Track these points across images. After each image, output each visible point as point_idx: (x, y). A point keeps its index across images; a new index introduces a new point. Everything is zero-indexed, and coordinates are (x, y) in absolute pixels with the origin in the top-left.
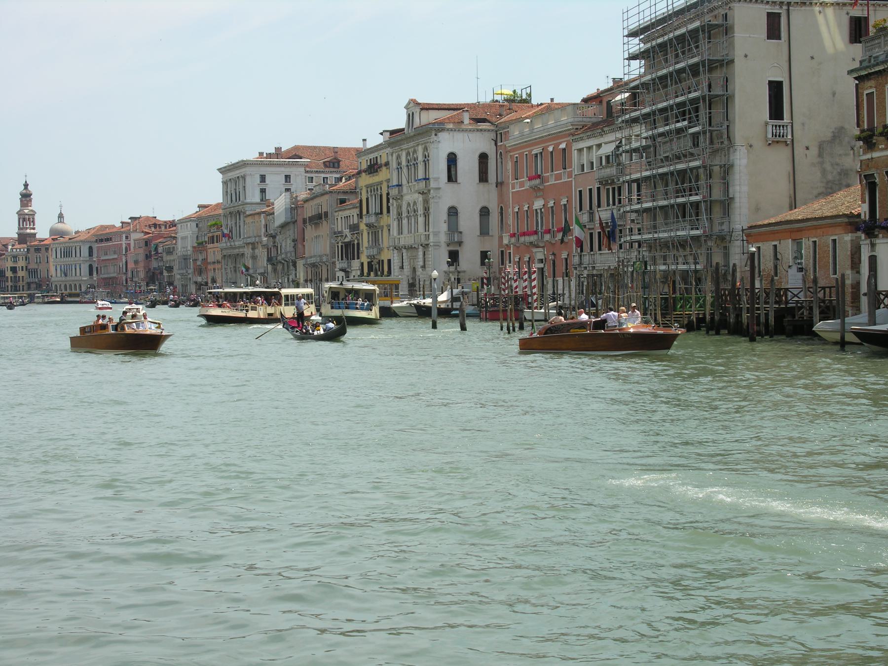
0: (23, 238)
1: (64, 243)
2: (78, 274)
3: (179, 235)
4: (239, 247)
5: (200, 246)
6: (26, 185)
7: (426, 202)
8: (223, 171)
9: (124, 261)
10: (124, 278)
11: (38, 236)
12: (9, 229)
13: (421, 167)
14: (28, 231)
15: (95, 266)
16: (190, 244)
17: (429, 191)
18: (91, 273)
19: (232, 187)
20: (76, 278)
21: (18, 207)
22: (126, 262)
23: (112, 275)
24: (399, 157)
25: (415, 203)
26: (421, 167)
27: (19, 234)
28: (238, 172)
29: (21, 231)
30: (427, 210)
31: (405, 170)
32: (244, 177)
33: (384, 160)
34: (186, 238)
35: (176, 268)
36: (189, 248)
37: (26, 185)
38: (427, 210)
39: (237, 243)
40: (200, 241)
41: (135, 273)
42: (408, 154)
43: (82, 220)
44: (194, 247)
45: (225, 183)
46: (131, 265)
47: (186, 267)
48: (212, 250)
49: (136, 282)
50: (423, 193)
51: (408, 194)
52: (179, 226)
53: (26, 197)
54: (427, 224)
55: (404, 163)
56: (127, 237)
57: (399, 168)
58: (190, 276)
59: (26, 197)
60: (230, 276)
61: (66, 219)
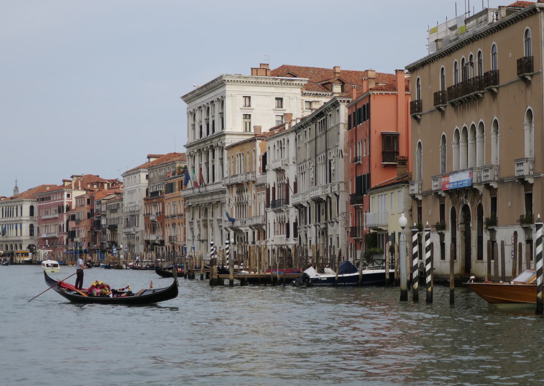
8: (188, 98)
20: (17, 238)
28: (213, 94)
56: (68, 196)
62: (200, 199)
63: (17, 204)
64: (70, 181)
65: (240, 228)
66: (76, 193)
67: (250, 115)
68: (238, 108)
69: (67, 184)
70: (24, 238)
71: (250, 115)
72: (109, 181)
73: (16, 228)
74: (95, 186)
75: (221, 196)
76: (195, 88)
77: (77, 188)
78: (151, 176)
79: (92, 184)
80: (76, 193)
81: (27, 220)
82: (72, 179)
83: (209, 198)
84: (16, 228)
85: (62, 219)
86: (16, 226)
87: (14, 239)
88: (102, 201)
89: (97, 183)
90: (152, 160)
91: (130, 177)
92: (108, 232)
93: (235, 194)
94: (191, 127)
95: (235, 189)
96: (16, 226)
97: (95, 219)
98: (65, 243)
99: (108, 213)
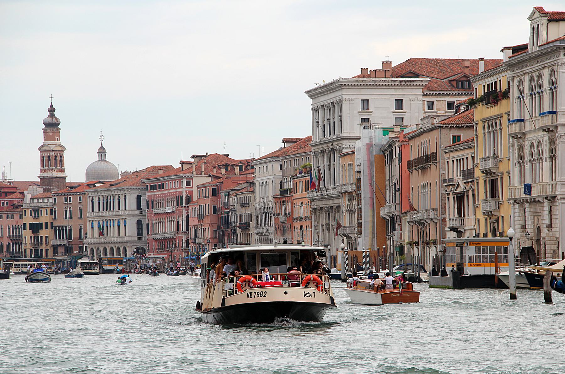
0: (45, 183)
1: (105, 187)
2: (122, 234)
3: (257, 181)
4: (333, 198)
5: (284, 194)
6: (52, 110)
7: (552, 141)
8: (313, 94)
9: (185, 216)
10: (184, 239)
11: (67, 180)
12: (25, 169)
13: (547, 97)
14: (55, 174)
15: (145, 222)
16: (272, 191)
17: (556, 127)
18: (139, 234)
19: (323, 115)
20: (119, 240)
21: (40, 140)
22: (187, 217)
23: (166, 235)
24: (521, 82)
25: (539, 143)
26: (547, 97)
27: (42, 178)
28: (332, 95)
29: (45, 174)
30: (553, 151)
31: (528, 101)
32: (340, 103)
33: (504, 87)
34: (266, 184)
35: (253, 225)
36: (271, 198)
37: (52, 110)
38: (553, 151)
39: (330, 192)
40: (285, 187)
41: (199, 232)
42: (532, 79)
43: (128, 160)
44: (275, 197)
45: (315, 111)
46: (194, 222)
47: (266, 223)
48: (298, 202)
49: (200, 244)
50: (548, 131)
51: (531, 131)
52: (257, 167)
53: (52, 126)
54: (553, 170)
55: (527, 91)
56: (188, 183)
57: (521, 98)
58: (271, 236)
59: (52, 126)
60: (321, 236)
61: (109, 157)
62: (324, 202)
63: (119, 192)
64: (190, 163)
65: (350, 235)
66: (198, 181)
67: (369, 119)
68: (356, 112)
69: (185, 167)
70: (129, 239)
71: (369, 119)
72: (241, 162)
73: (119, 226)
74: (223, 171)
75: (336, 201)
76: (317, 86)
77: (199, 174)
78: (284, 168)
79: (219, 167)
80: (198, 181)
81: (133, 215)
82: (192, 160)
83: (331, 202)
84: (119, 226)
85: (181, 213)
86: (119, 222)
87: (115, 240)
88: (231, 193)
89: (226, 166)
90: (287, 145)
91: (262, 166)
92: (239, 231)
93: (347, 202)
94: (315, 124)
95: (347, 197)
96: (119, 222)
97: (223, 215)
98: (184, 245)
99: (238, 207)
